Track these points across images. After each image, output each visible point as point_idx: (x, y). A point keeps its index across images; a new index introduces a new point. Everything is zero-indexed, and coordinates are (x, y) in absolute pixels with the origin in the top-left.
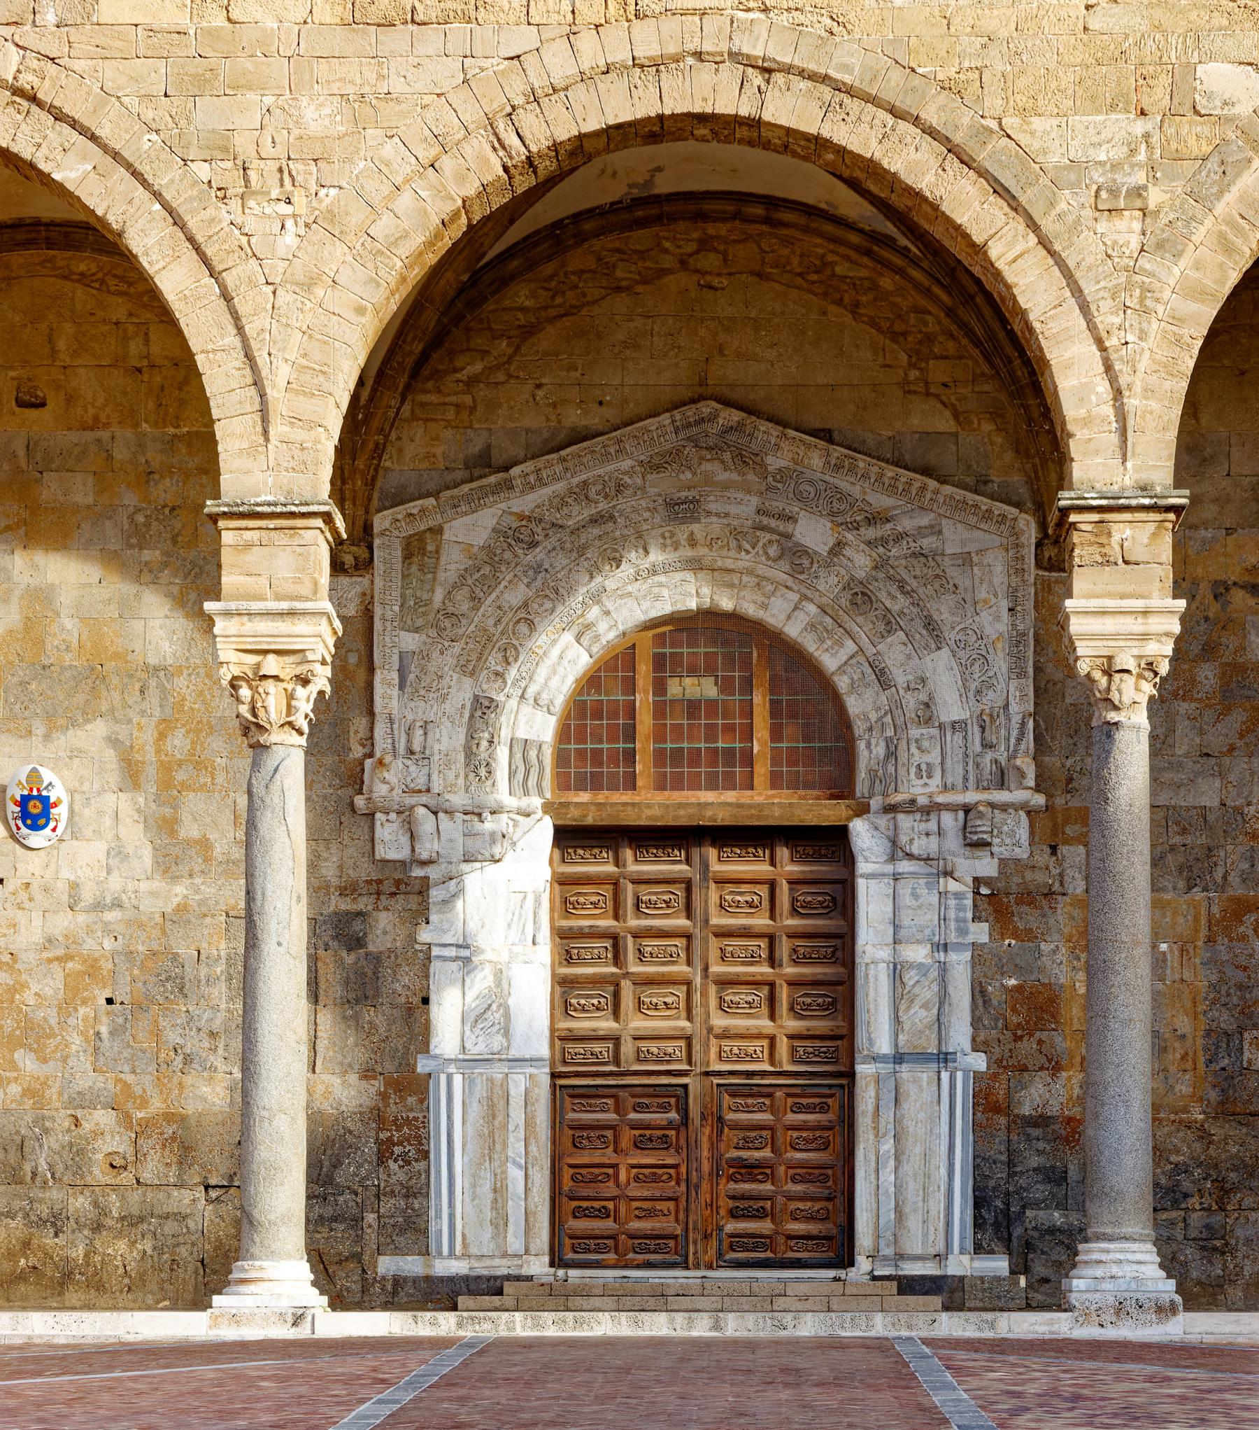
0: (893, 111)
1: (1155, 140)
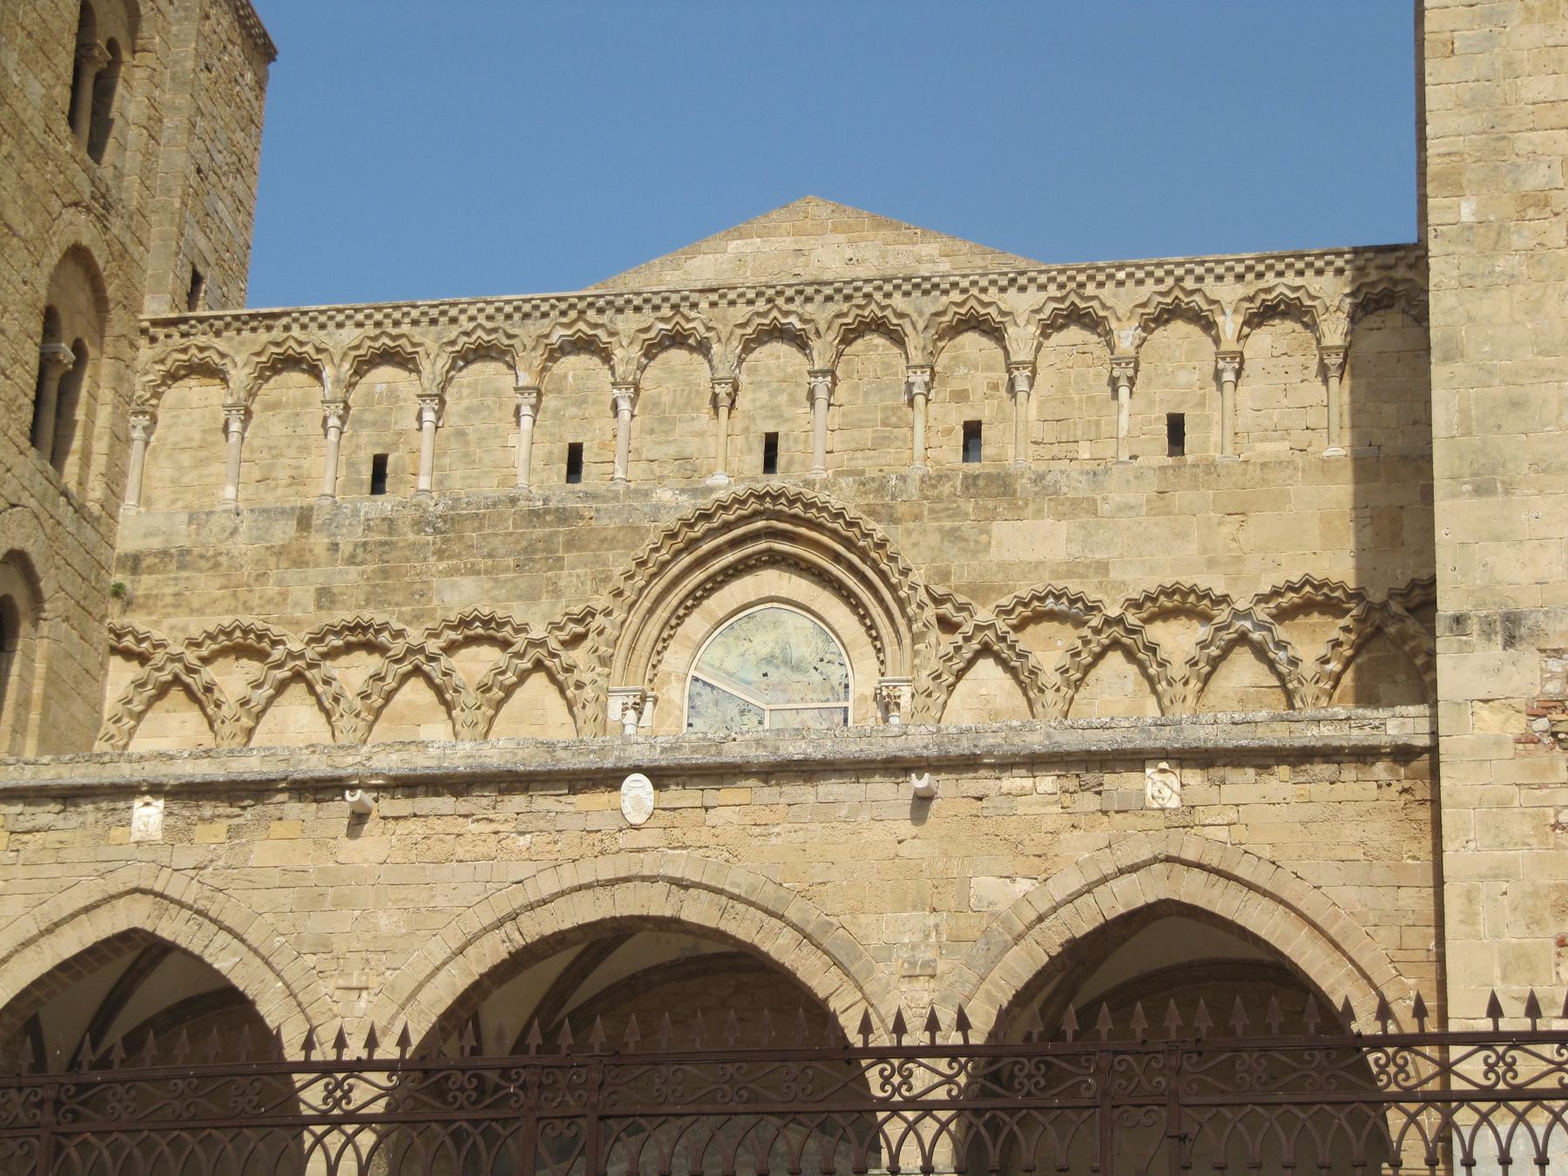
0: (767, 911)
1: (942, 928)
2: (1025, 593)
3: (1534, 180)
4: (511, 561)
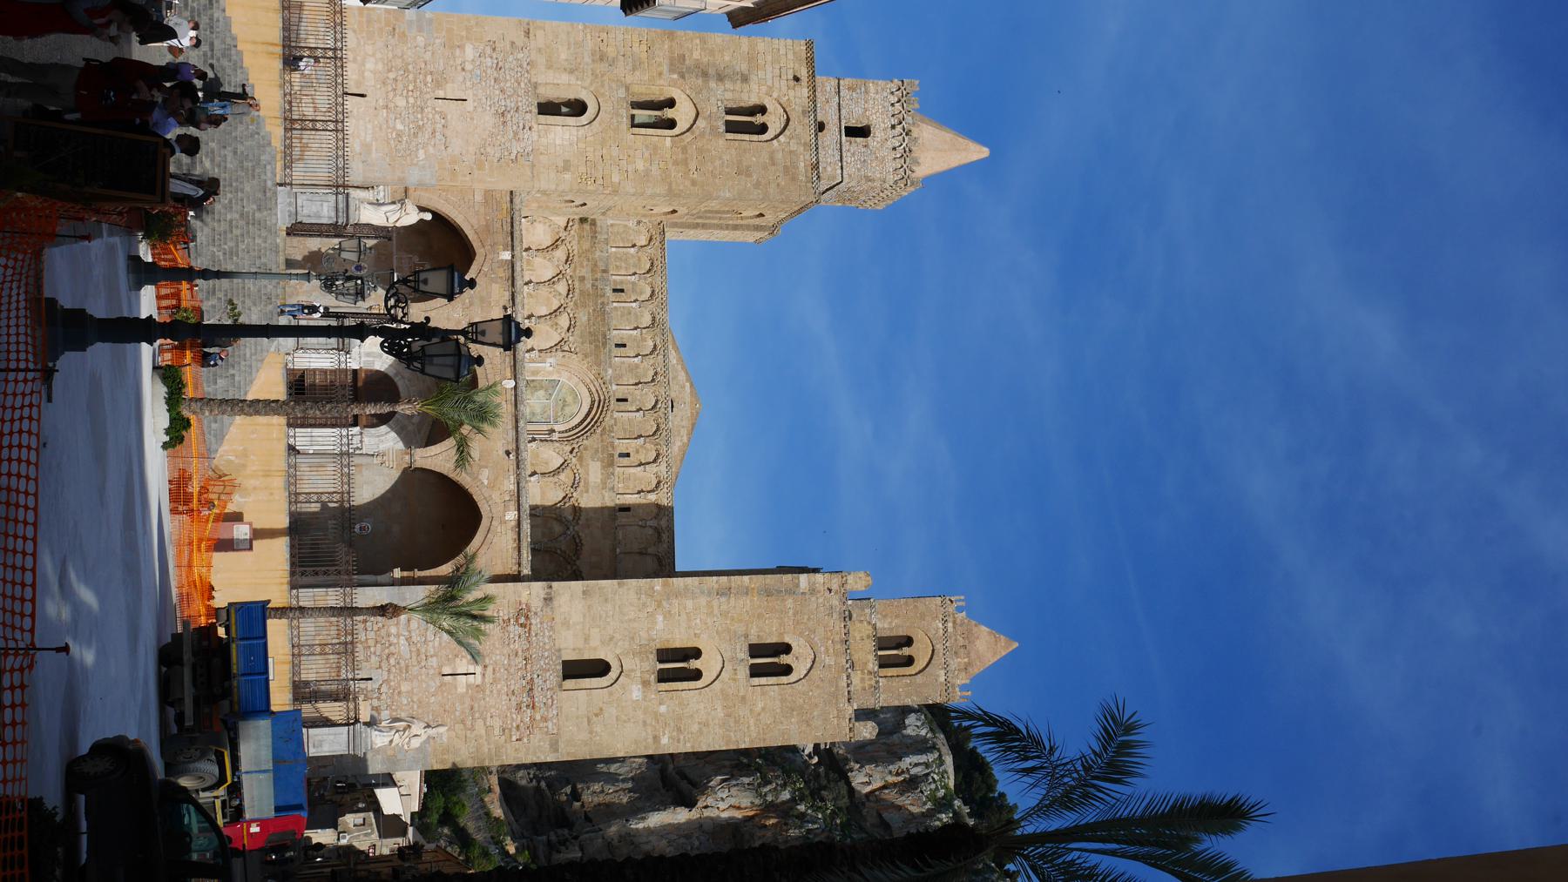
3: (664, 603)
4: (592, 330)
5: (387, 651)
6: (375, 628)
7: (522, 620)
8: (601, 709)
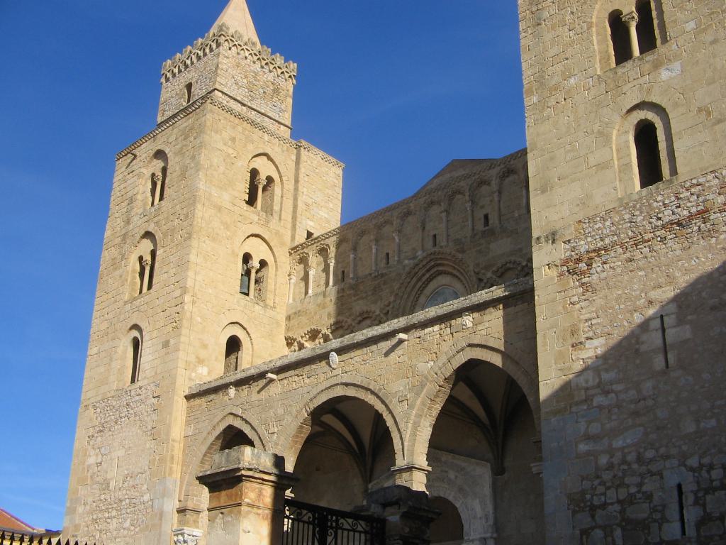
2: (500, 265)
5: (635, 466)
6: (601, 489)
7: (583, 266)
8: (700, 110)
